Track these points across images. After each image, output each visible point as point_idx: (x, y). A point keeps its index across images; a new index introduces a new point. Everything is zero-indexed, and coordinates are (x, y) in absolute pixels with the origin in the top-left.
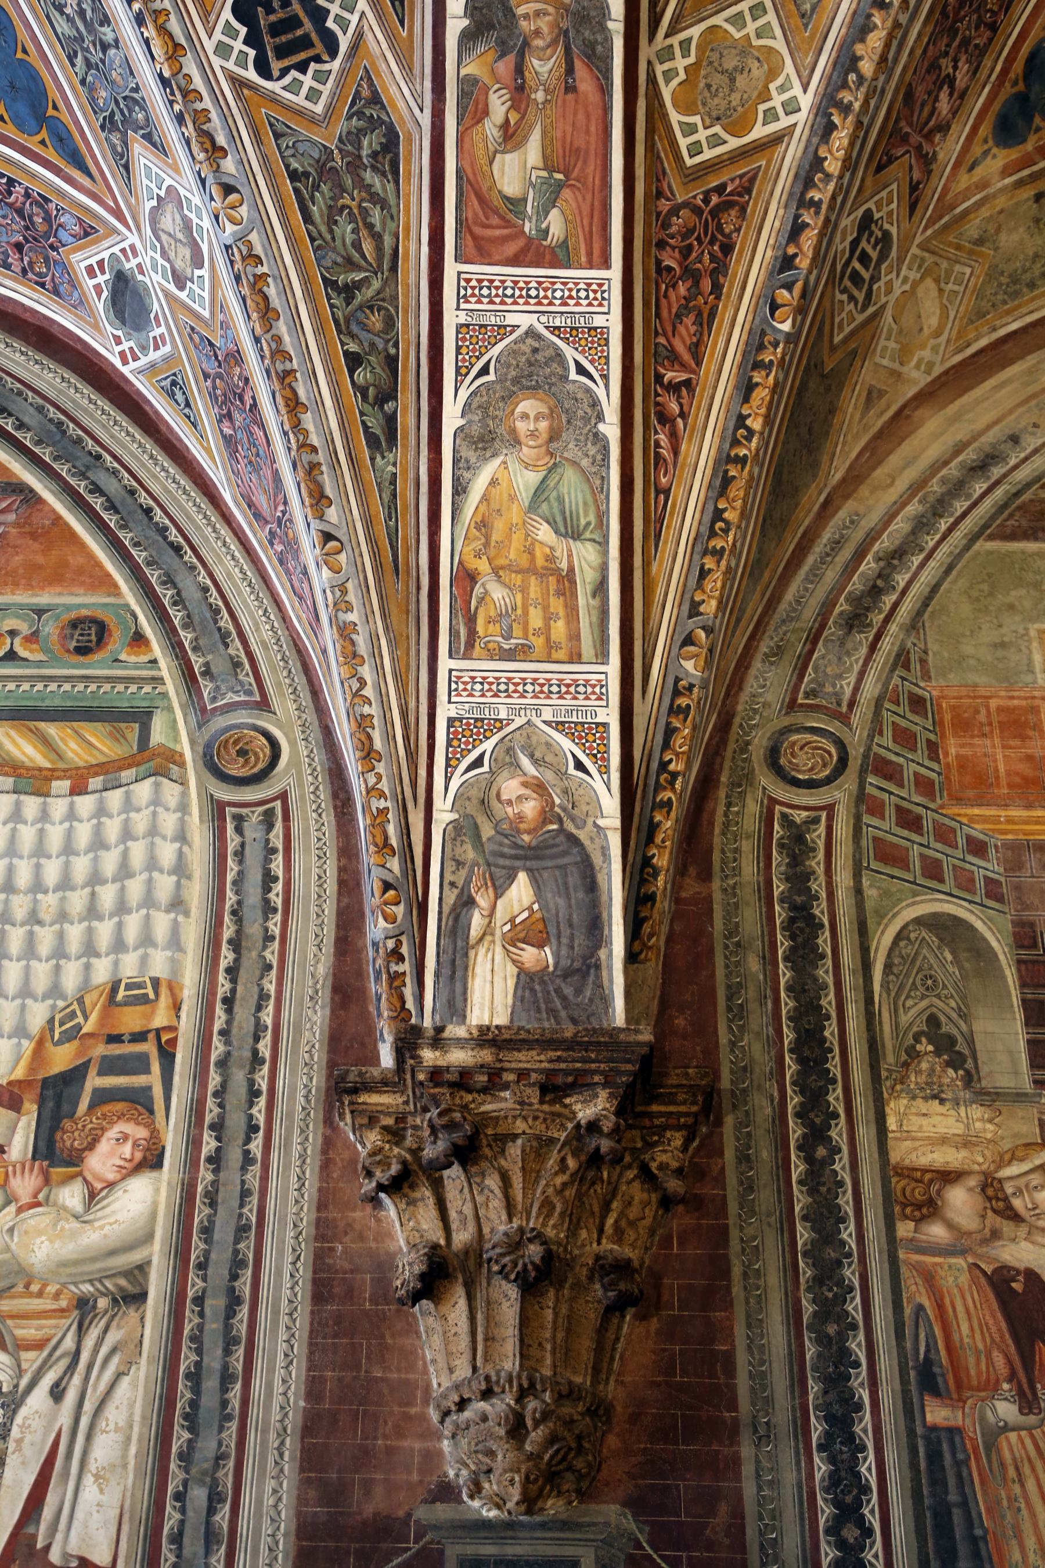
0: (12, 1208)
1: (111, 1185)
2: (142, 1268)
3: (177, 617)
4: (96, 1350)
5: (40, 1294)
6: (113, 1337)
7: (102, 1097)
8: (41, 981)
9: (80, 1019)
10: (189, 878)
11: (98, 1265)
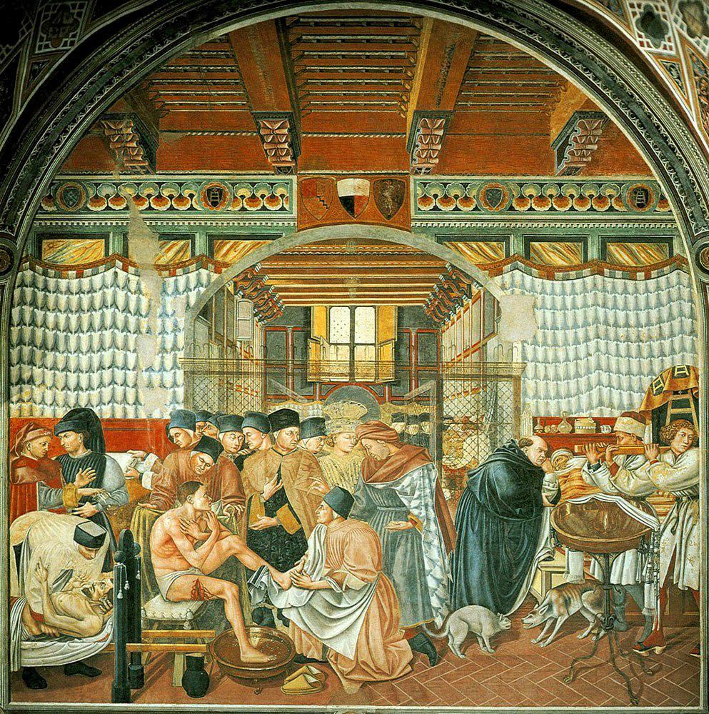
0: (648, 463)
1: (682, 453)
2: (697, 485)
3: (677, 186)
4: (684, 517)
5: (663, 496)
6: (689, 512)
7: (674, 417)
8: (646, 370)
9: (662, 384)
10: (696, 320)
11: (681, 485)
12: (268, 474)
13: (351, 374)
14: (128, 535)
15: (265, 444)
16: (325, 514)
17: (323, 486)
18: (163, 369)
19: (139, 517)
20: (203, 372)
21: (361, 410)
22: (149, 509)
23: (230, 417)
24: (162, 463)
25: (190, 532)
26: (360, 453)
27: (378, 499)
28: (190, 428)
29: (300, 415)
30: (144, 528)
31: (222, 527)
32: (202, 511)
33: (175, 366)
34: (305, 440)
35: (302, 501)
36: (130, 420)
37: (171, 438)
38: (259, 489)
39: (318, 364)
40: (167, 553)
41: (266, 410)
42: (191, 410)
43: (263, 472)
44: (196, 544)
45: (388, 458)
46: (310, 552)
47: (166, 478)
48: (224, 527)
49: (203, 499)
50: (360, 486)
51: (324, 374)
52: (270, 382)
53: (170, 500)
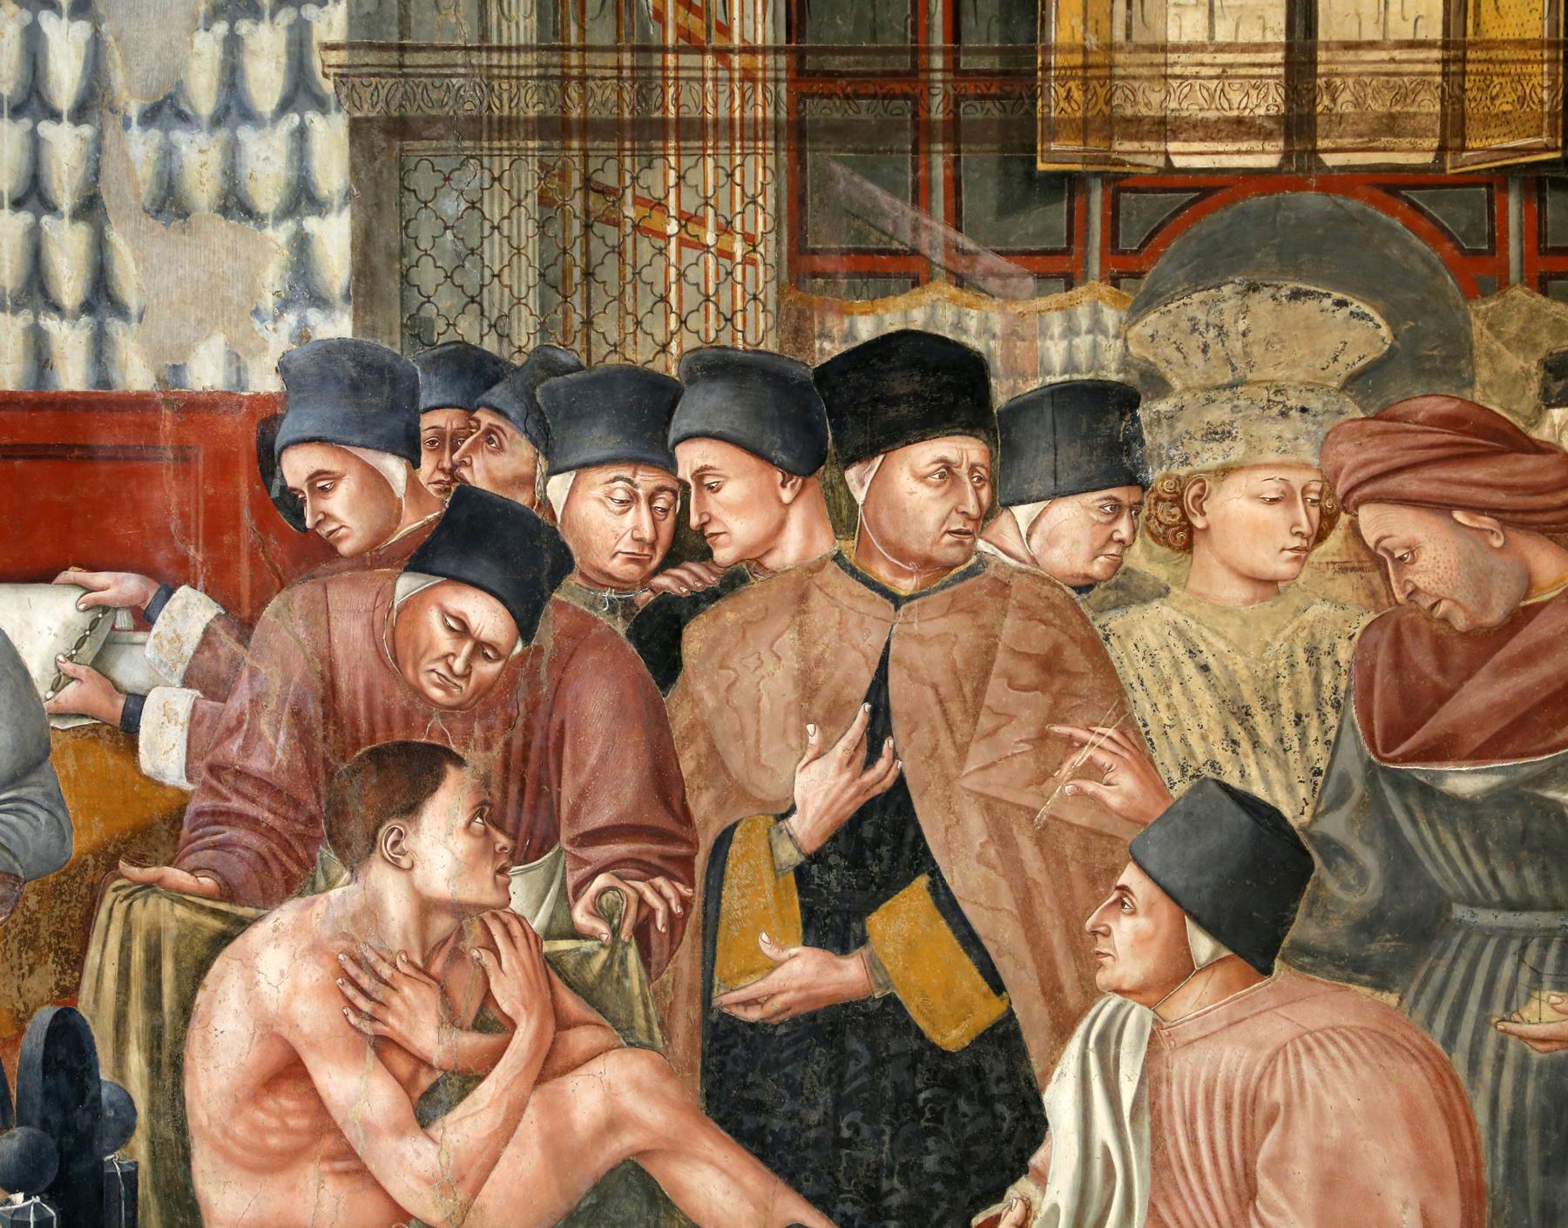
12: (815, 702)
13: (1297, 125)
14: (69, 1043)
15: (801, 538)
16: (1141, 941)
17: (1126, 781)
18: (234, 106)
19: (125, 949)
20: (450, 122)
21: (1360, 333)
22: (178, 895)
23: (608, 380)
24: (244, 638)
25: (395, 1025)
26: (1344, 587)
27: (1447, 859)
28: (391, 448)
29: (997, 364)
30: (153, 1002)
31: (571, 1004)
32: (459, 910)
33: (300, 91)
34: (1023, 513)
35: (1013, 865)
36: (69, 404)
37: (291, 504)
38: (769, 788)
39: (1097, 70)
40: (274, 1141)
41: (798, 331)
42: (390, 343)
43: (792, 695)
44: (430, 1097)
45: (1520, 618)
46: (1060, 1154)
47: (264, 726)
48: (578, 995)
49: (462, 844)
50: (1345, 780)
51: (1136, 127)
52: (828, 179)
53: (288, 848)
